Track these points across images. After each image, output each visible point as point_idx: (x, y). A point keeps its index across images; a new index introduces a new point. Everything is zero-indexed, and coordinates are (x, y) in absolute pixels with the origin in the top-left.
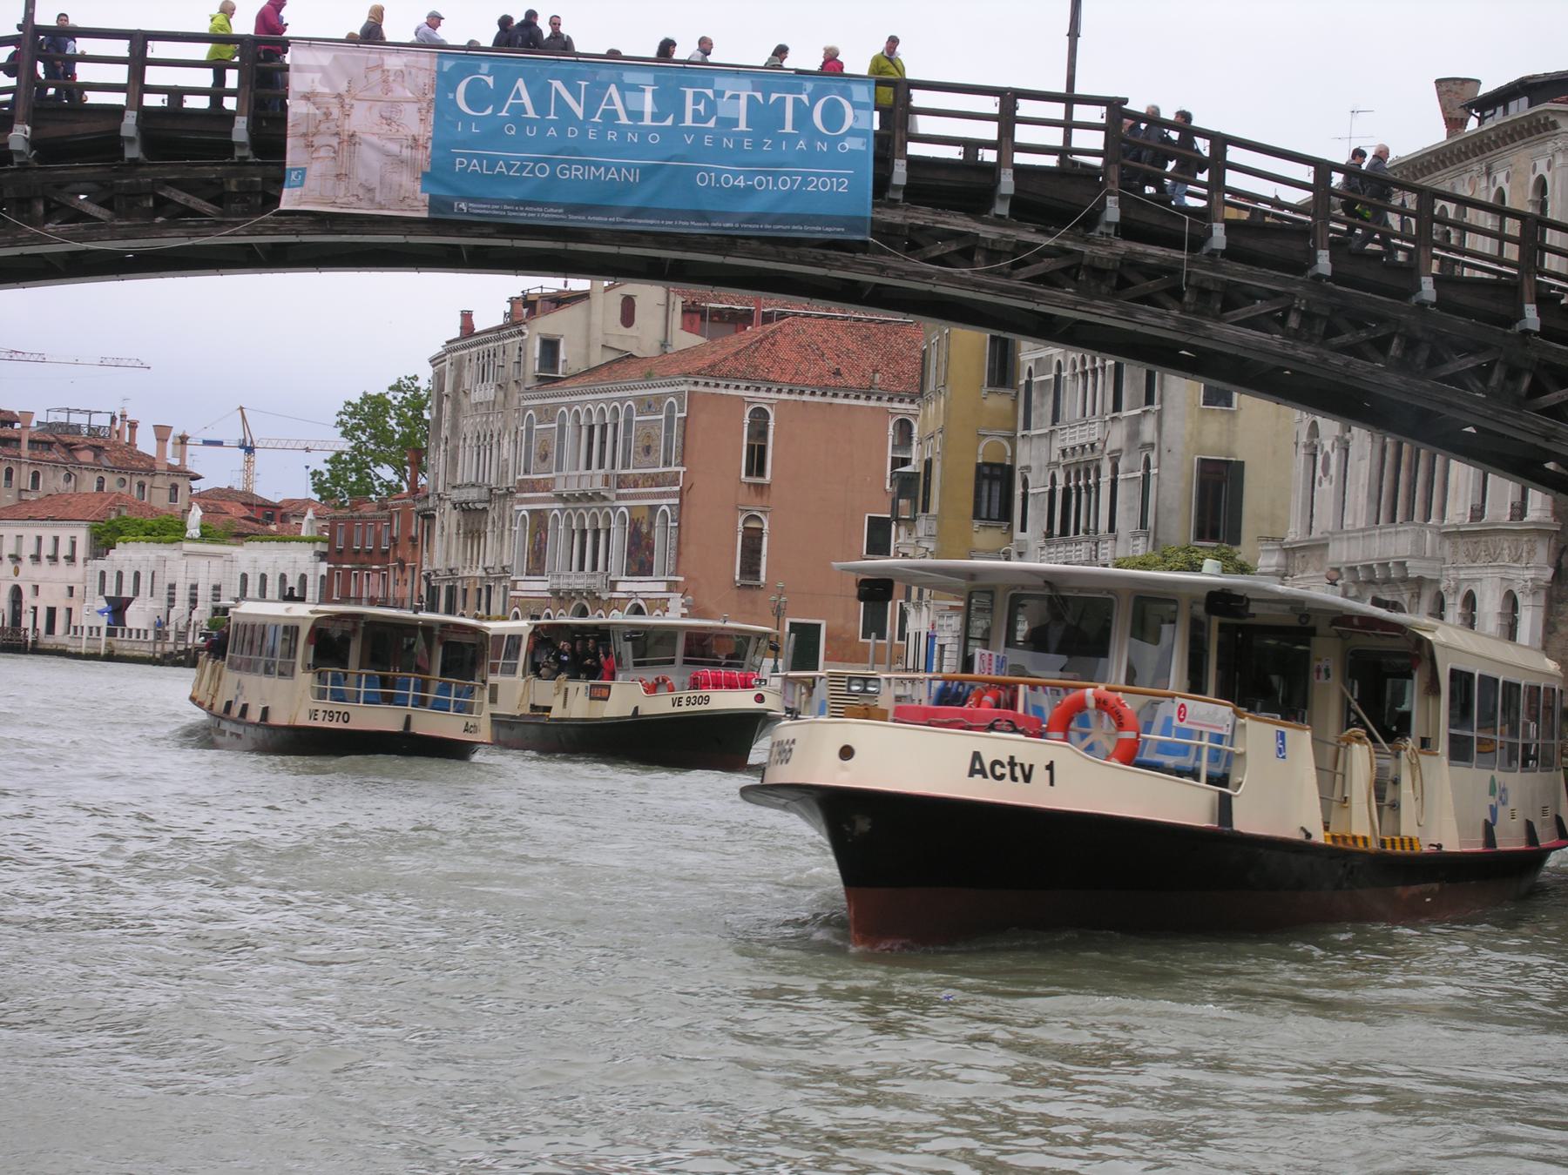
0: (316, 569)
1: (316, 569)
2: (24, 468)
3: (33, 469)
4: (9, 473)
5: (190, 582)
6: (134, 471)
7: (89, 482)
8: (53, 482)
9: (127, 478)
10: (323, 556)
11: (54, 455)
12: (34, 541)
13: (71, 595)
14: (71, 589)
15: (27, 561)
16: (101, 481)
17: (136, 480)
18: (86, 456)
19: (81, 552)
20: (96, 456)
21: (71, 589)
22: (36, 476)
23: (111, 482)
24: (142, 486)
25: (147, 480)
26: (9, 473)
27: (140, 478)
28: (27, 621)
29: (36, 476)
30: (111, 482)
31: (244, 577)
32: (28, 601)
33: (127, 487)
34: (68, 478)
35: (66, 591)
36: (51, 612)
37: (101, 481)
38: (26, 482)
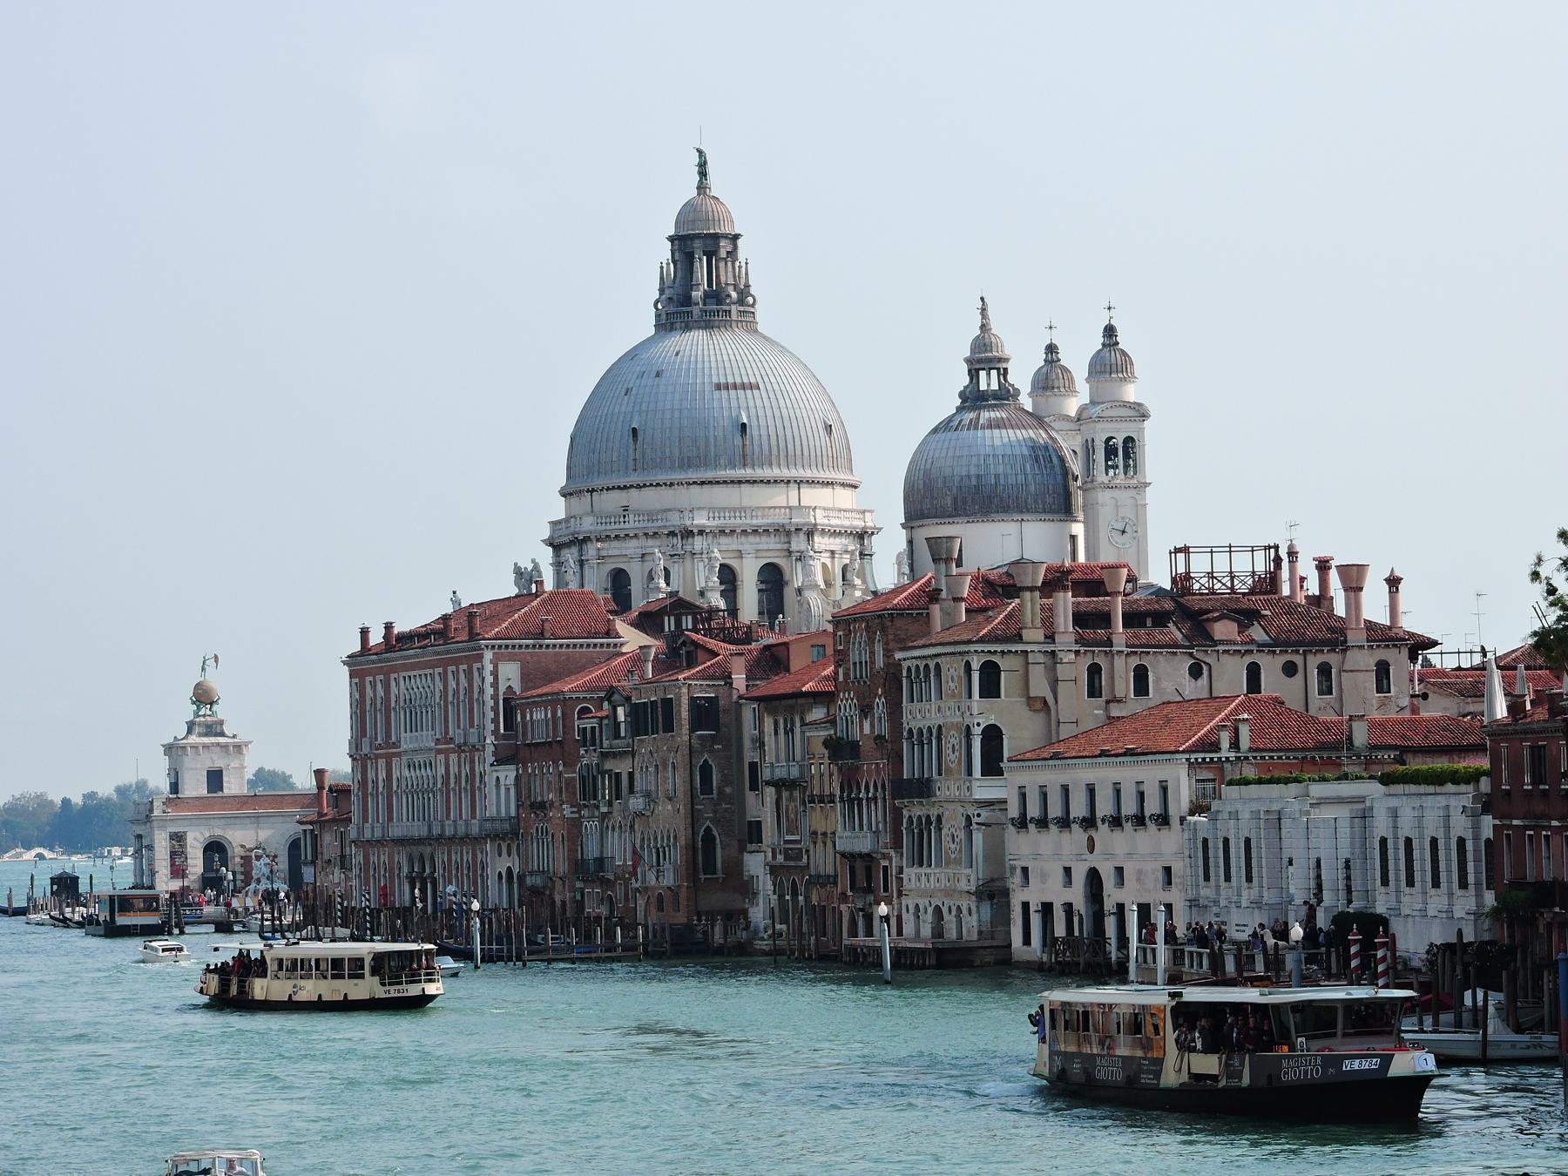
0: (1476, 828)
1: (1476, 828)
2: (1119, 662)
3: (1134, 661)
5: (1313, 855)
6: (1310, 645)
7: (1230, 674)
8: (1171, 677)
9: (1298, 659)
10: (1487, 805)
11: (1174, 632)
12: (1110, 791)
13: (1170, 883)
14: (1168, 870)
15: (1104, 828)
16: (1254, 672)
17: (1314, 661)
18: (1224, 629)
19: (1174, 812)
20: (1243, 628)
21: (1168, 870)
22: (1141, 675)
23: (1271, 668)
24: (1325, 670)
25: (1333, 659)
26: (1094, 671)
27: (1320, 658)
28: (1110, 925)
29: (1141, 675)
30: (1271, 668)
31: (1383, 841)
32: (1112, 895)
33: (1299, 676)
34: (1195, 672)
35: (1160, 875)
36: (1144, 910)
37: (1254, 672)
38: (1124, 684)
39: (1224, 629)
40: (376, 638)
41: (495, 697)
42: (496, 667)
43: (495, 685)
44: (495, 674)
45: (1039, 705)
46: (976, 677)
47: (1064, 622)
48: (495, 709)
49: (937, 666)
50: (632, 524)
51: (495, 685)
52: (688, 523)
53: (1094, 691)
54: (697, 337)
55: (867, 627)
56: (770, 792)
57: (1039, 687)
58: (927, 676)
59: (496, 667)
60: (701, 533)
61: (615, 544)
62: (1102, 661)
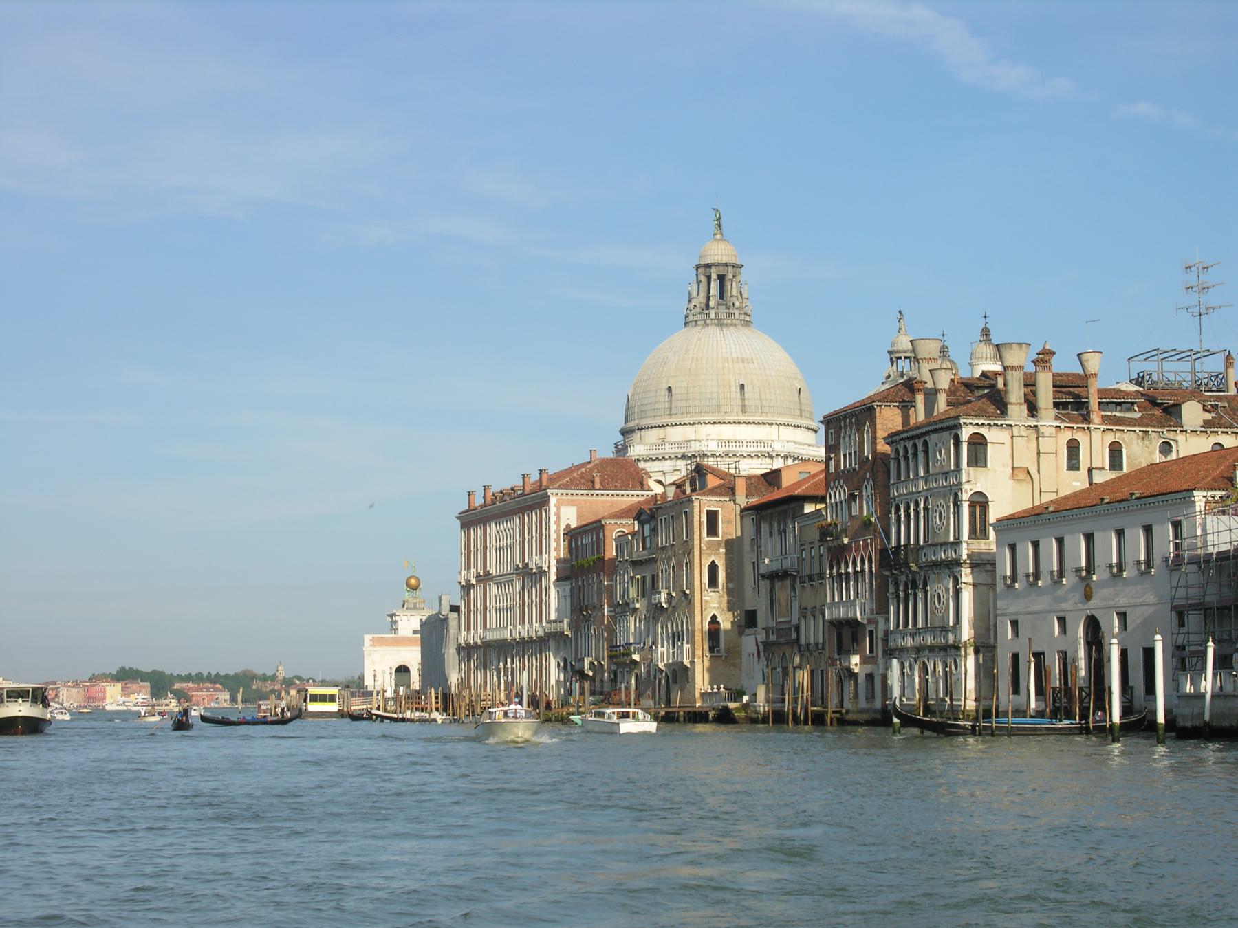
2: (1096, 435)
3: (1110, 438)
4: (1073, 447)
26: (1073, 447)
34: (1166, 448)
39: (1192, 413)
40: (478, 501)
41: (557, 532)
42: (558, 509)
43: (558, 523)
44: (558, 515)
45: (1022, 475)
46: (965, 447)
47: (1046, 396)
48: (557, 540)
49: (926, 444)
50: (668, 449)
51: (558, 523)
52: (704, 449)
53: (1073, 464)
54: (713, 331)
55: (857, 420)
56: (765, 584)
57: (1026, 459)
58: (915, 455)
59: (558, 509)
60: (713, 455)
61: (656, 463)
62: (1079, 436)
